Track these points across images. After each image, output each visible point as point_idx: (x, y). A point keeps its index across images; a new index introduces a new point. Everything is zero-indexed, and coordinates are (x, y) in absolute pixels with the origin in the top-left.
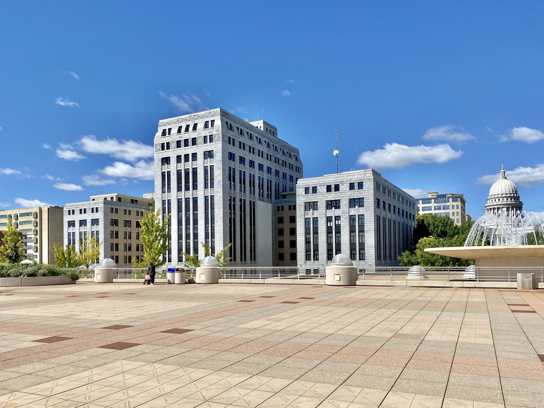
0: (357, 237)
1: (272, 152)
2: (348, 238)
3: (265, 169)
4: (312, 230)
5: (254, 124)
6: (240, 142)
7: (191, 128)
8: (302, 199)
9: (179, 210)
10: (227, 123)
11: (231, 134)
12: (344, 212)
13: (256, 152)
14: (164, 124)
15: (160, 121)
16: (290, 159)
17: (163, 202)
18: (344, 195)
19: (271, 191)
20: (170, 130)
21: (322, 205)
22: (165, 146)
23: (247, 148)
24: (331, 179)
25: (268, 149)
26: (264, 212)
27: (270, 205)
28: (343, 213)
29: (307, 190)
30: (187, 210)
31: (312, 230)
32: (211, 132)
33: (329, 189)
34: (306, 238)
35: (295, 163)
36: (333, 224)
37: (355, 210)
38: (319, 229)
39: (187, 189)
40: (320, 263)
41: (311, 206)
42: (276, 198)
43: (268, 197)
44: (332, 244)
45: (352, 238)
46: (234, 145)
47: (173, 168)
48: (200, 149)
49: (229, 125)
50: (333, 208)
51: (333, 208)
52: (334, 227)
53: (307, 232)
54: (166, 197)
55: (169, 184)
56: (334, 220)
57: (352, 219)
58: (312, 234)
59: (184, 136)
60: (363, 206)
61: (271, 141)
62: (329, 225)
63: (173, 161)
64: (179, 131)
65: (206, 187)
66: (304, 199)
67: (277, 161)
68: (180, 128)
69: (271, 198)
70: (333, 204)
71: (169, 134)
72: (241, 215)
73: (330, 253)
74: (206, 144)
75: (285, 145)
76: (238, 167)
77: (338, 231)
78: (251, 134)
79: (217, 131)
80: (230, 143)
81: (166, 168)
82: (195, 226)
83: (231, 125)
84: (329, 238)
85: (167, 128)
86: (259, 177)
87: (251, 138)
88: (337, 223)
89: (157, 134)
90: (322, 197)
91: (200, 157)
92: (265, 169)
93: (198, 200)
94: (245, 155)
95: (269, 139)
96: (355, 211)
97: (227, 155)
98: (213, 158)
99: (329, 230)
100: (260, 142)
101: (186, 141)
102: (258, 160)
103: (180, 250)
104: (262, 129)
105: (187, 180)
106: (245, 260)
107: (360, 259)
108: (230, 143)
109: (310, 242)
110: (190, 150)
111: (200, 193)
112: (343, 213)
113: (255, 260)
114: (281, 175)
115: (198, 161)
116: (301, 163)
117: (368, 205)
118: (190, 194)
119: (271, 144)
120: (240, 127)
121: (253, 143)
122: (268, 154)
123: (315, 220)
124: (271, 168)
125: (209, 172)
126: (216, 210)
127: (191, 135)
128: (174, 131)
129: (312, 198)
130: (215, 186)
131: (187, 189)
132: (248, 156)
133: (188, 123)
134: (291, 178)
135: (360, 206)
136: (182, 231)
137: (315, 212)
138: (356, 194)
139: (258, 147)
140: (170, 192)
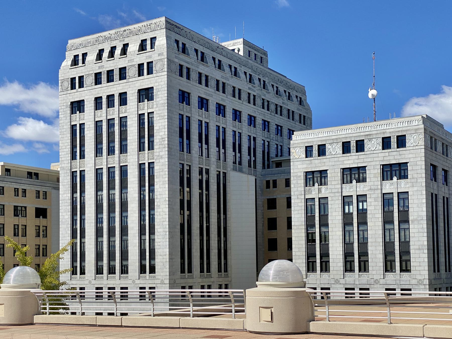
0: (397, 231)
1: (256, 91)
2: (380, 232)
3: (245, 118)
4: (317, 219)
5: (229, 45)
6: (200, 74)
7: (118, 52)
8: (299, 167)
10: (177, 42)
11: (183, 60)
12: (373, 188)
13: (229, 90)
14: (75, 46)
15: (70, 42)
16: (289, 102)
17: (73, 174)
18: (374, 158)
19: (255, 156)
20: (85, 55)
21: (334, 177)
22: (77, 83)
23: (212, 83)
24: (351, 132)
25: (250, 85)
26: (243, 191)
27: (252, 179)
28: (371, 189)
29: (308, 151)
31: (317, 219)
32: (150, 57)
33: (346, 148)
34: (308, 234)
35: (298, 109)
36: (353, 209)
37: (392, 184)
38: (330, 218)
39: (111, 151)
40: (332, 276)
41: (317, 177)
42: (264, 167)
43: (250, 166)
44: (353, 243)
45: (387, 234)
46: (188, 78)
47: (88, 117)
48: (132, 86)
49: (181, 45)
50: (354, 181)
51: (354, 181)
52: (355, 214)
53: (310, 223)
54: (78, 165)
55: (82, 145)
56: (355, 201)
57: (386, 200)
58: (317, 226)
59: (107, 65)
60: (406, 177)
61: (255, 72)
62: (347, 211)
63: (89, 106)
64: (99, 57)
65: (141, 148)
66: (305, 166)
67: (266, 105)
68: (101, 51)
69: (255, 167)
70: (355, 174)
71: (83, 62)
72: (201, 195)
73: (349, 259)
74: (141, 78)
75: (280, 79)
76: (195, 114)
77: (363, 222)
78: (220, 61)
79: (159, 55)
80: (181, 75)
81: (77, 119)
82: (124, 214)
83: (184, 45)
84: (346, 233)
85: (80, 52)
86: (235, 132)
87: (220, 66)
88: (361, 207)
89: (64, 64)
90: (335, 162)
91: (132, 98)
92: (245, 118)
94: (209, 95)
95: (251, 68)
96: (393, 186)
97: (176, 95)
98: (152, 99)
99: (347, 220)
100: (236, 74)
101: (110, 74)
102: (231, 104)
103: (99, 256)
104: (241, 53)
105: (111, 138)
106: (209, 270)
107: (402, 270)
108: (181, 75)
109: (314, 241)
110: (116, 88)
111: (132, 159)
112: (371, 189)
113: (226, 271)
114: (273, 128)
116: (308, 110)
117: (415, 176)
118: (115, 161)
119: (256, 77)
120: (201, 49)
121: (223, 76)
122: (249, 94)
123: (324, 203)
124: (255, 117)
125: (145, 124)
126: (157, 187)
128: (92, 57)
129: (317, 163)
130: (155, 147)
131: (111, 151)
132: (215, 98)
134: (279, 129)
135: (400, 178)
136: (102, 222)
137: (323, 188)
138: (394, 156)
139: (232, 82)
140: (84, 158)
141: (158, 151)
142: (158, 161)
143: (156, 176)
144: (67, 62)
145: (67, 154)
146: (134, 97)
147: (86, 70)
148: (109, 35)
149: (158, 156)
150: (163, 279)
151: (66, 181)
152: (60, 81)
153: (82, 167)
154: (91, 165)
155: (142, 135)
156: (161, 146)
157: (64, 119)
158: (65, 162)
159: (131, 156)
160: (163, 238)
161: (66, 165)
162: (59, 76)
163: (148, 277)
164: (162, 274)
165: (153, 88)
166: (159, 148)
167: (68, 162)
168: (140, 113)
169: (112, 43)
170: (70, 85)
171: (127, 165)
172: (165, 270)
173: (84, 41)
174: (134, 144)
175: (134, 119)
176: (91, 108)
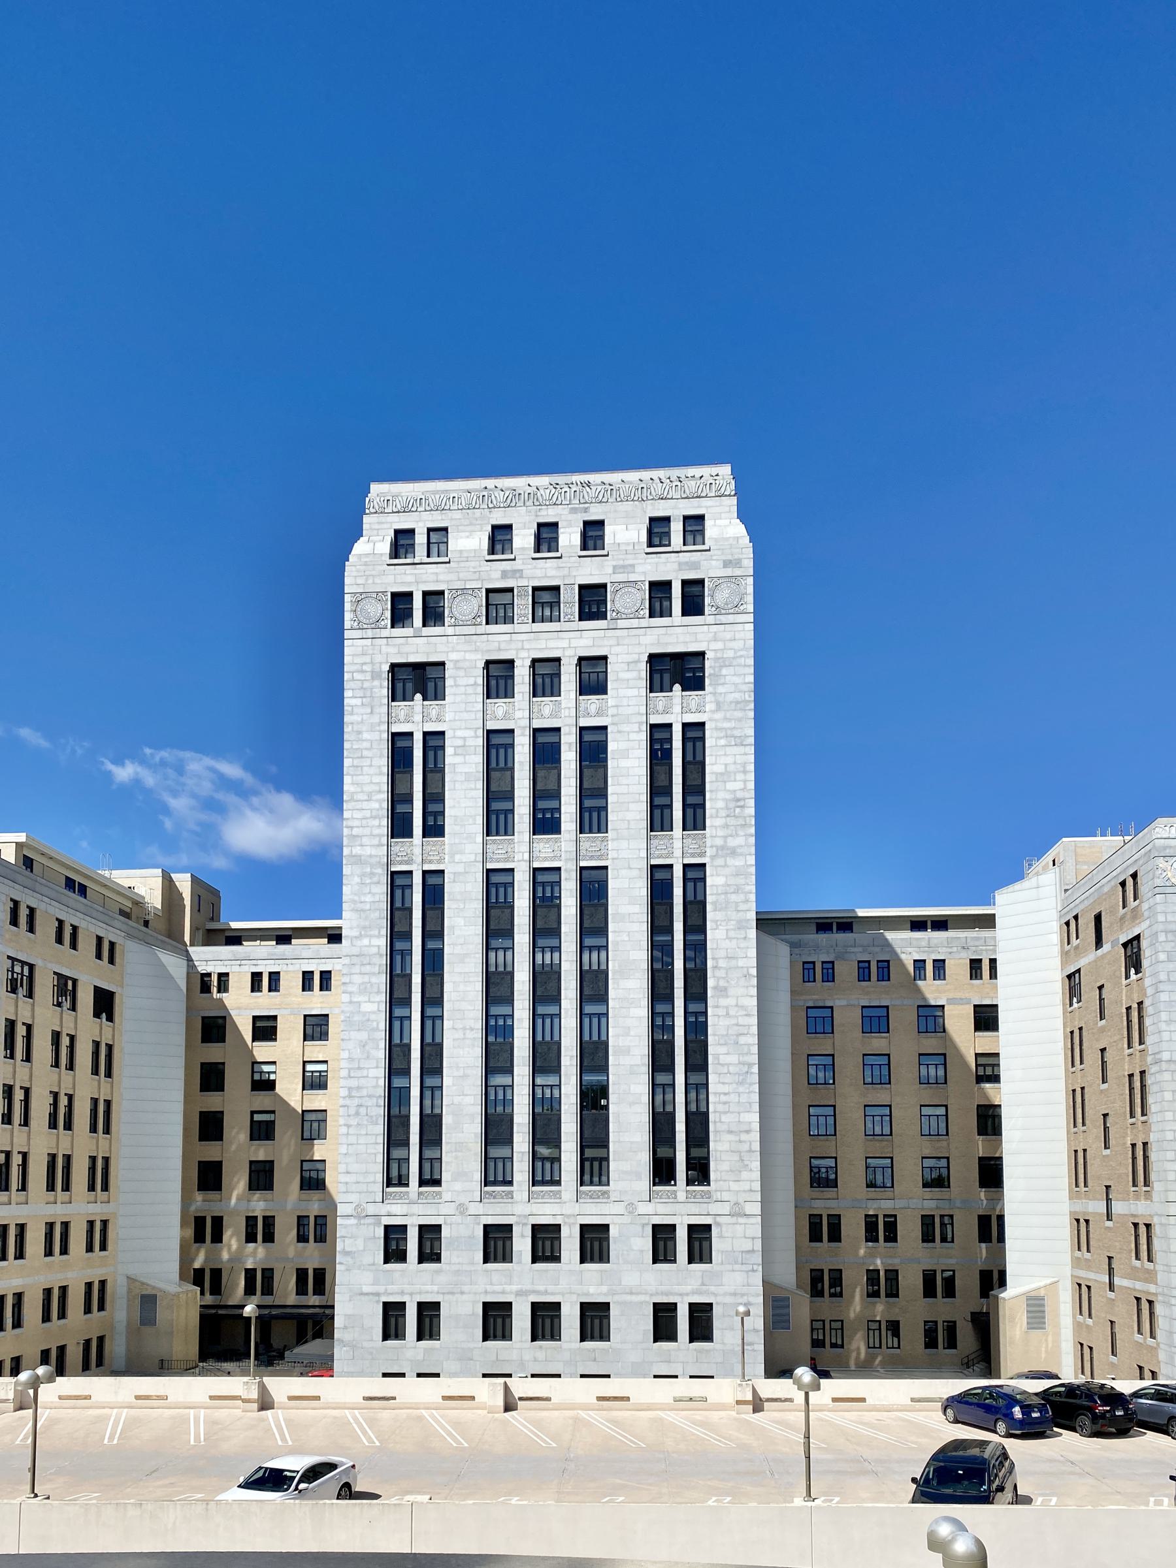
9: (497, 929)
15: (377, 489)
17: (398, 882)
20: (437, 535)
30: (545, 930)
39: (545, 823)
47: (462, 716)
54: (415, 854)
59: (527, 569)
65: (658, 819)
81: (415, 717)
89: (359, 548)
93: (612, 884)
110: (570, 640)
115: (611, 697)
118: (564, 851)
126: (715, 935)
127: (571, 569)
131: (545, 823)
133: (548, 516)
141: (721, 833)
142: (720, 861)
143: (714, 903)
144: (373, 544)
145: (374, 818)
146: (634, 674)
147: (452, 577)
148: (529, 490)
149: (722, 848)
150: (741, 1201)
151: (368, 898)
152: (347, 598)
153: (430, 862)
154: (472, 858)
155: (661, 781)
156: (731, 821)
157: (362, 710)
158: (365, 840)
159: (624, 844)
160: (741, 1083)
161: (368, 851)
162: (347, 581)
163: (681, 1196)
164: (734, 1186)
165: (702, 654)
166: (726, 826)
167: (376, 841)
168: (655, 720)
169: (543, 513)
170: (388, 614)
171: (606, 868)
172: (745, 1175)
173: (435, 492)
174: (632, 806)
175: (633, 736)
176: (470, 690)
